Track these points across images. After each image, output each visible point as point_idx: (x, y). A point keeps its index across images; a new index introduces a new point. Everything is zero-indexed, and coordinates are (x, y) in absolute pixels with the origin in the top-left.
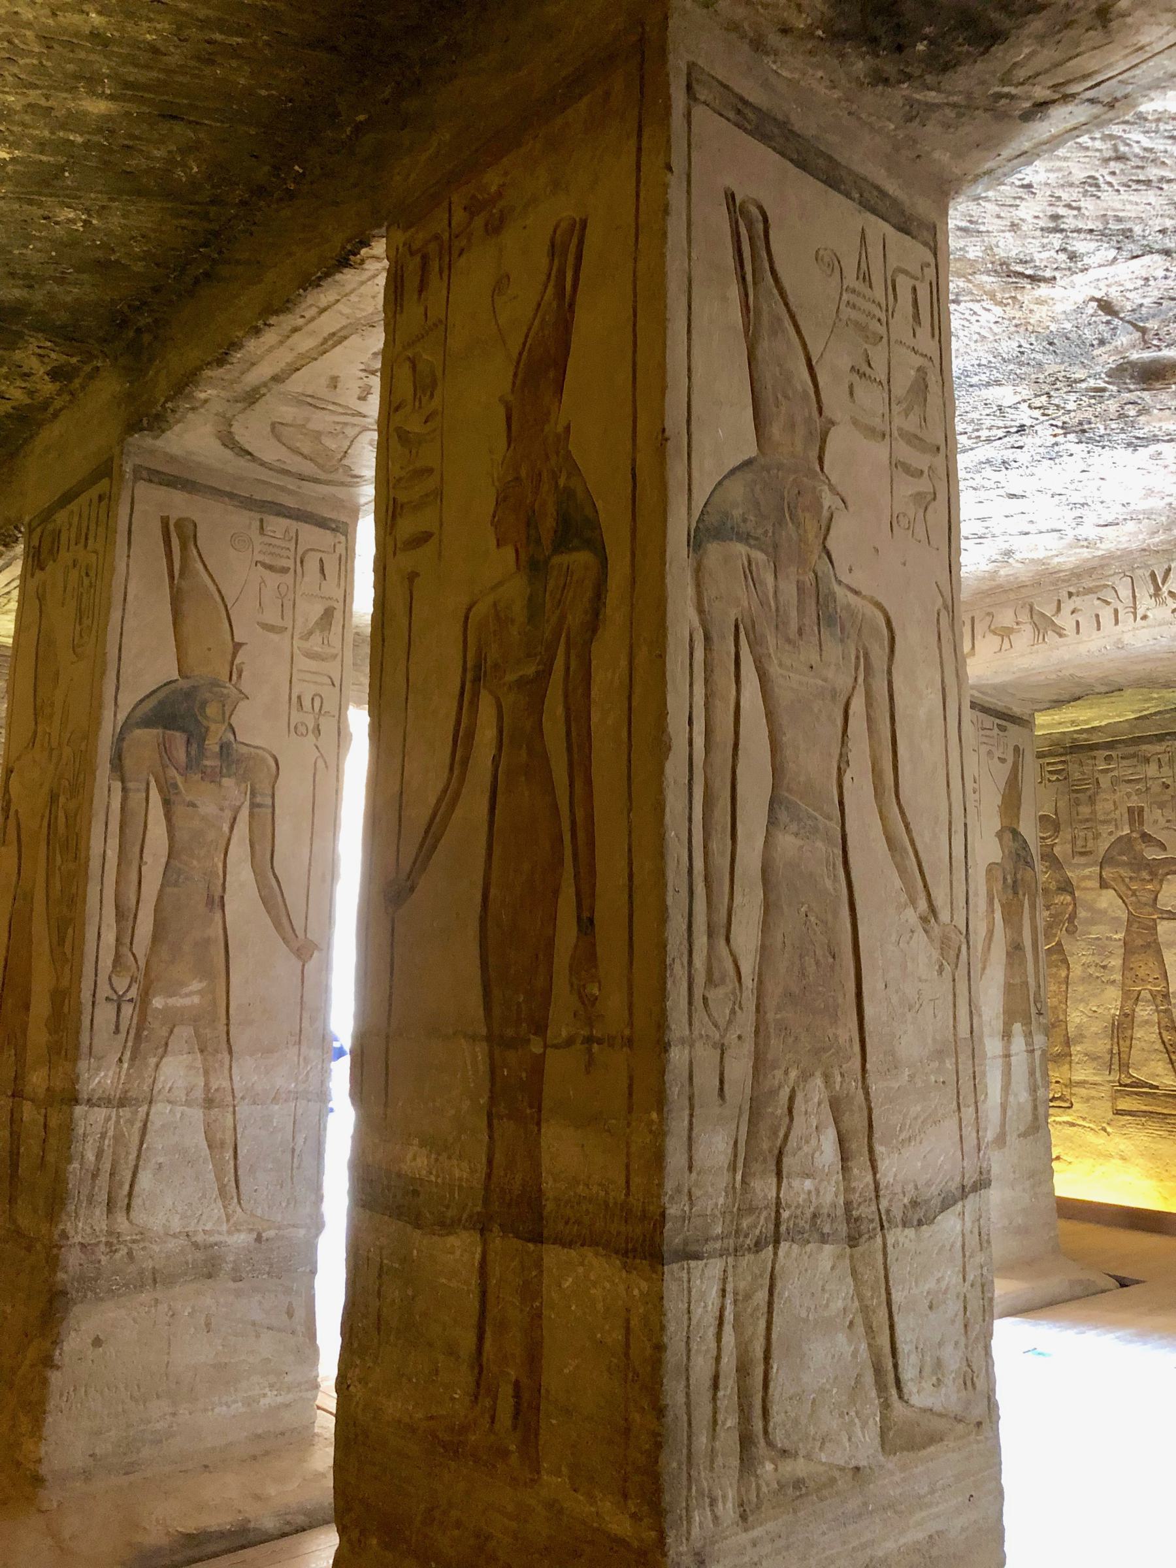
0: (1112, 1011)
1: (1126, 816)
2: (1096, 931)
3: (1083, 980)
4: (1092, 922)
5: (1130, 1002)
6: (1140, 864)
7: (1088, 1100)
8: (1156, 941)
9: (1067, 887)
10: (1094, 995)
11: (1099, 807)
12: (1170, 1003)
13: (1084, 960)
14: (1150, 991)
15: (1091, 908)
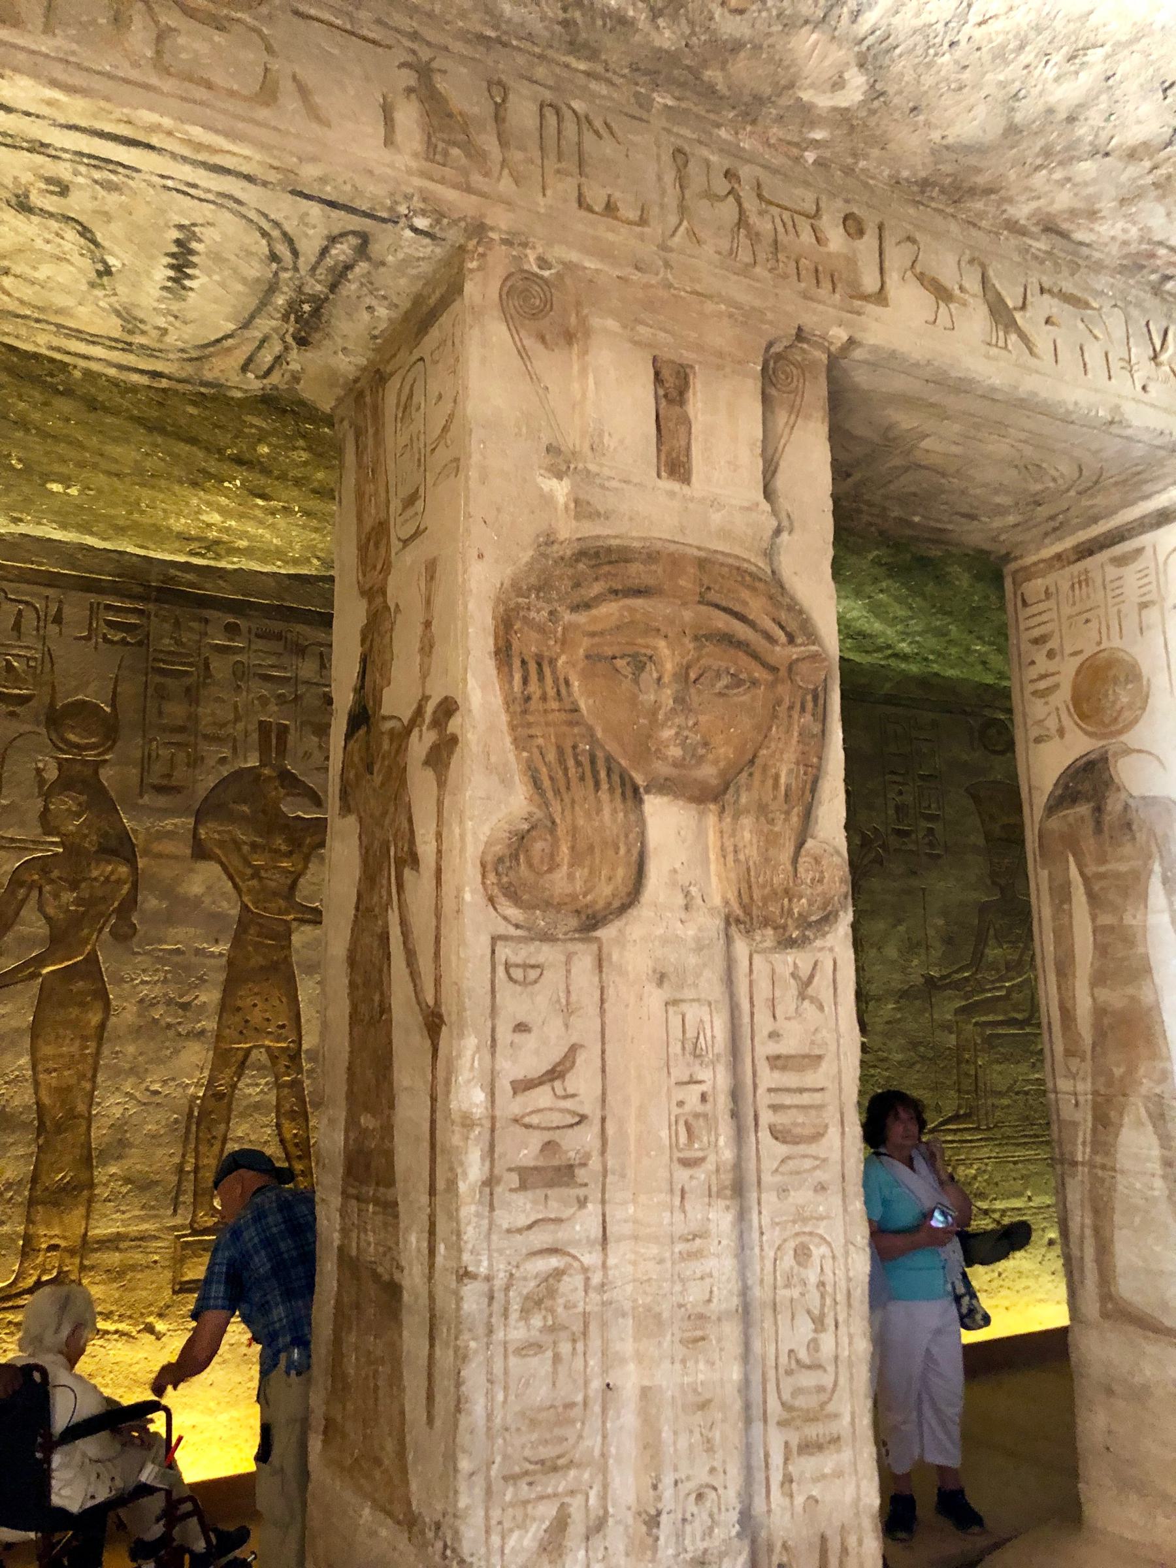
0: (192, 1090)
1: (255, 736)
2: (179, 937)
3: (137, 1032)
4: (170, 919)
5: (229, 1071)
6: (272, 823)
7: (121, 1274)
8: (287, 960)
9: (120, 847)
10: (161, 1061)
11: (205, 711)
12: (300, 1070)
13: (145, 991)
14: (268, 1048)
15: (168, 892)
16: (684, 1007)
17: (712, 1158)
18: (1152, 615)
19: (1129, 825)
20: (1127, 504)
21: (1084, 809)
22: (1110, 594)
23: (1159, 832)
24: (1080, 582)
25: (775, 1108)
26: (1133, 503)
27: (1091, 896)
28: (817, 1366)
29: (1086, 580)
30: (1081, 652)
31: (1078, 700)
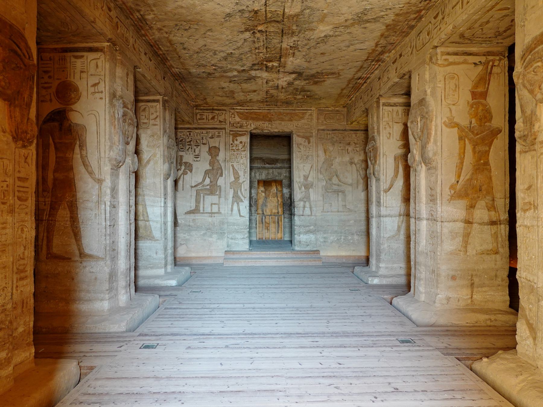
16: (4, 160)
17: (8, 203)
18: (84, 75)
19: (70, 130)
20: (81, 42)
21: (56, 124)
22: (72, 66)
23: (80, 133)
24: (62, 59)
25: (18, 191)
26: (83, 43)
27: (56, 148)
28: (23, 259)
29: (64, 59)
30: (60, 79)
31: (58, 93)
